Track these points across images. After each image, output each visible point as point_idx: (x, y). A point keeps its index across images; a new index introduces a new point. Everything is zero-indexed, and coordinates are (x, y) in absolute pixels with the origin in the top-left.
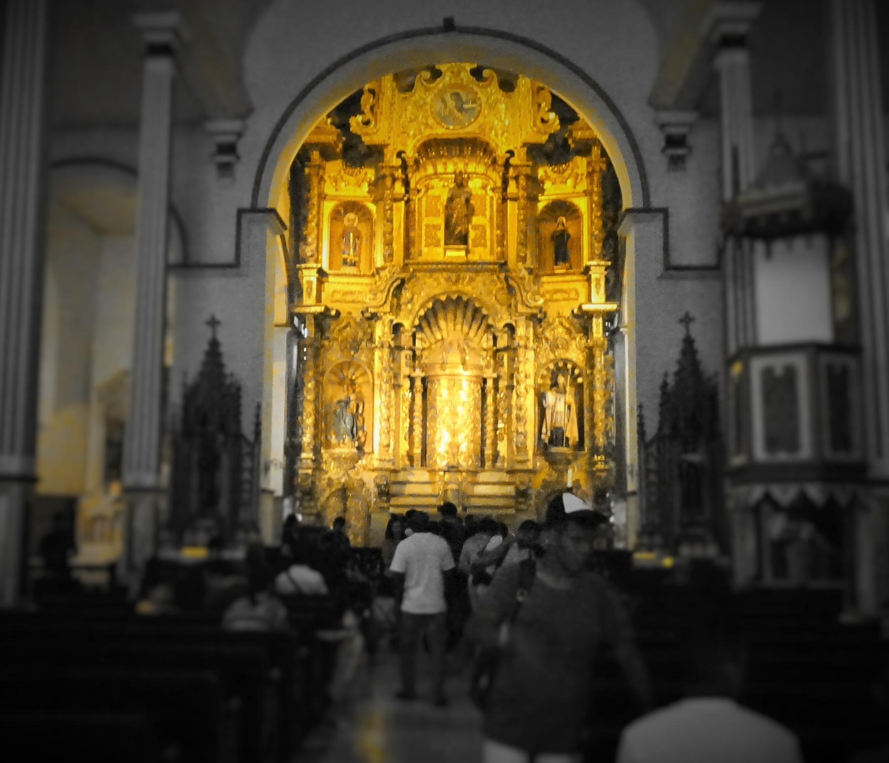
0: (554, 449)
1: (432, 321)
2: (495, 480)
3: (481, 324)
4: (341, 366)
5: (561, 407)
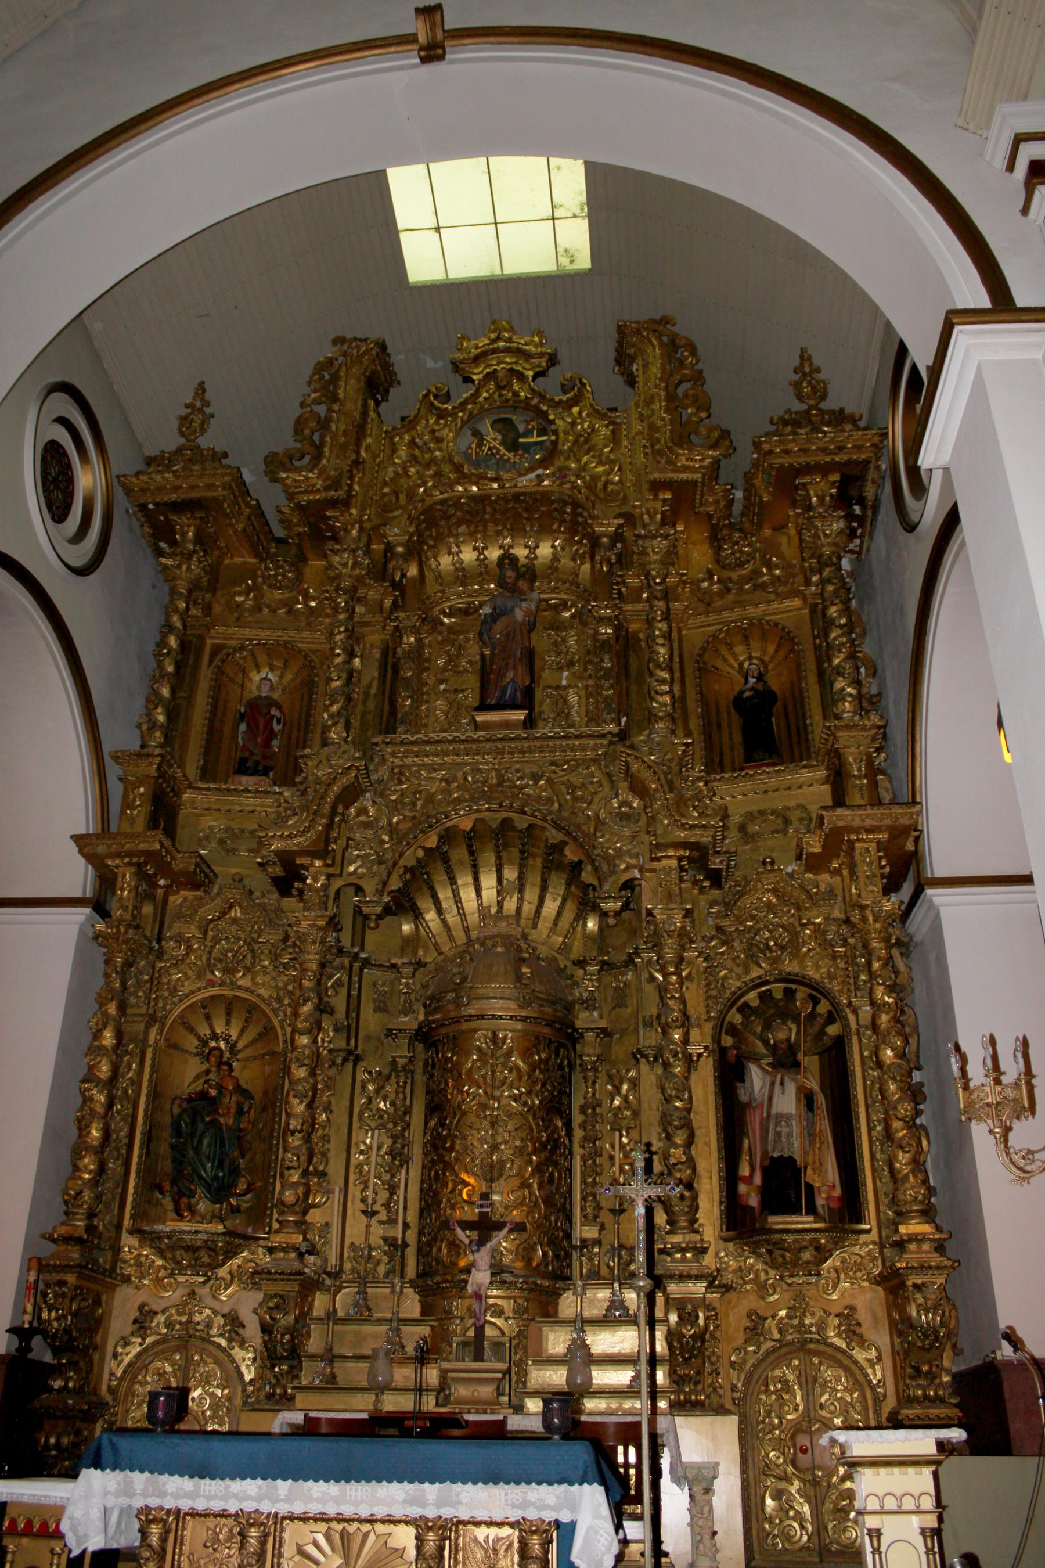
0: (776, 1221)
1: (444, 894)
5: (786, 1102)
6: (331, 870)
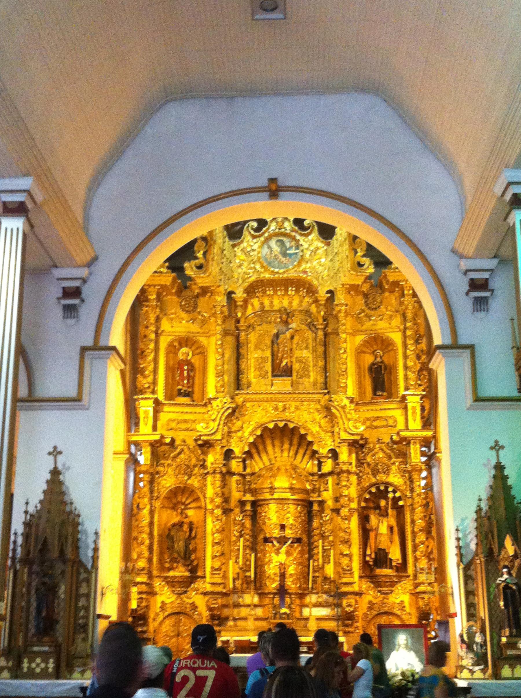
0: (378, 571)
1: (261, 447)
3: (306, 450)
5: (383, 529)
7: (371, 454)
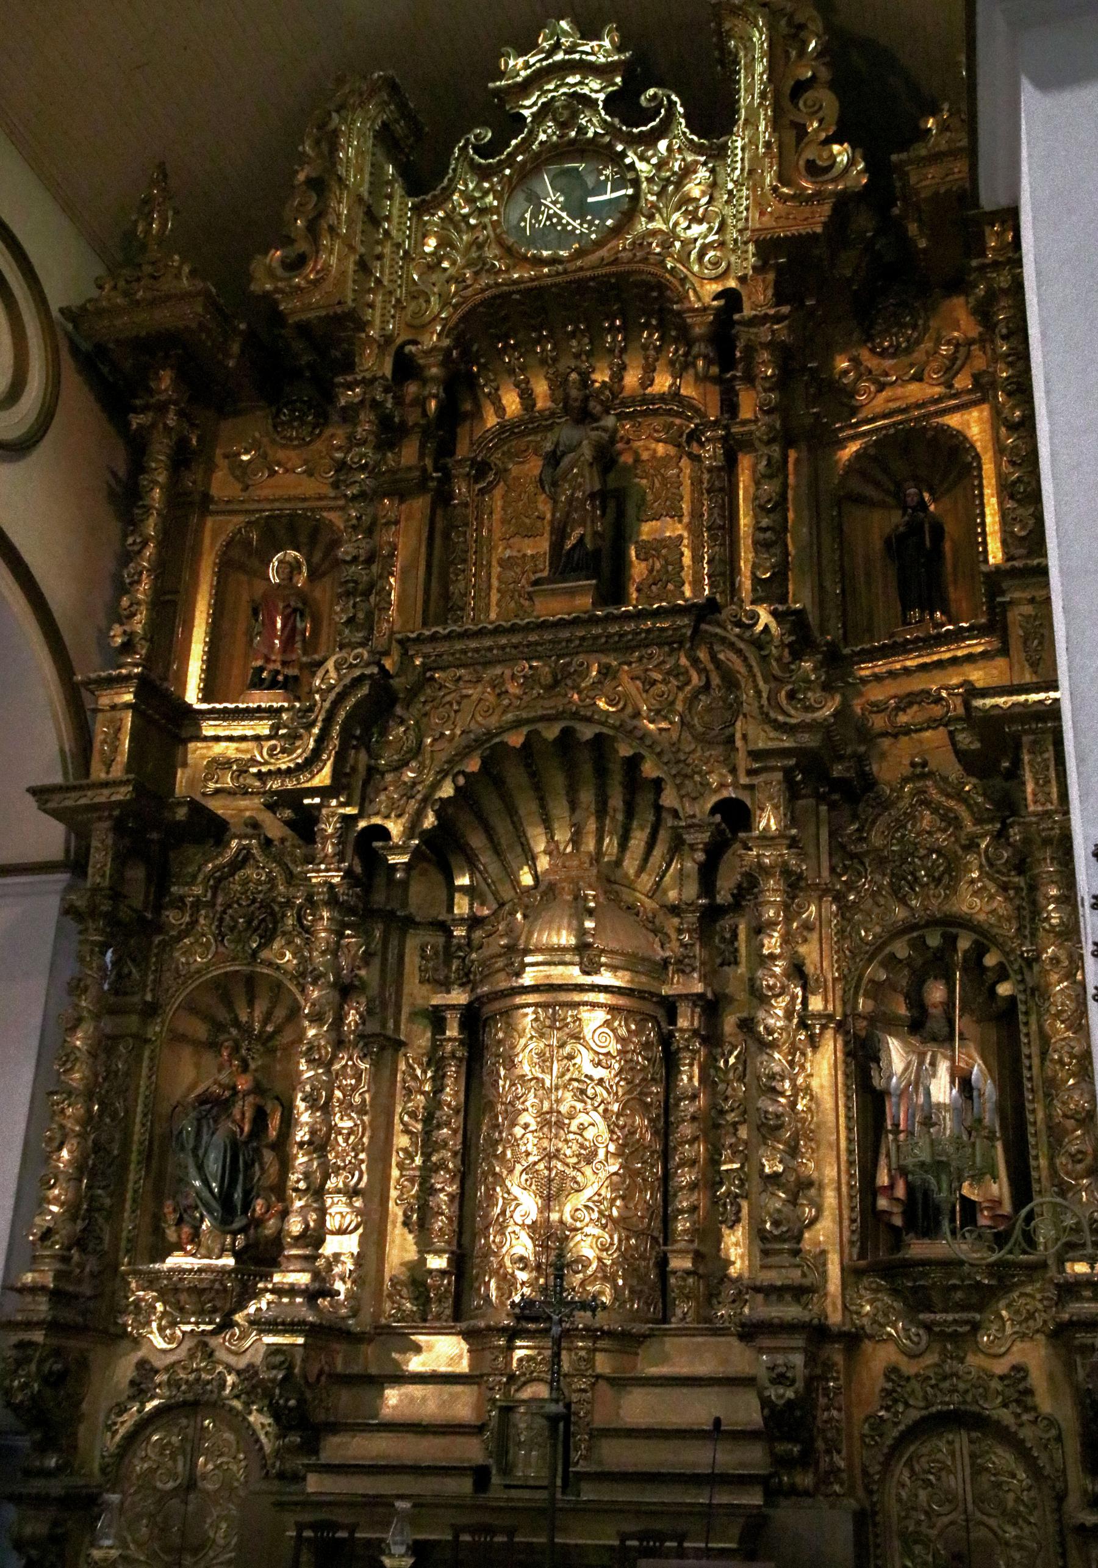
0: (919, 1249)
1: (503, 828)
2: (702, 1369)
4: (222, 988)
6: (349, 811)
7: (885, 818)
